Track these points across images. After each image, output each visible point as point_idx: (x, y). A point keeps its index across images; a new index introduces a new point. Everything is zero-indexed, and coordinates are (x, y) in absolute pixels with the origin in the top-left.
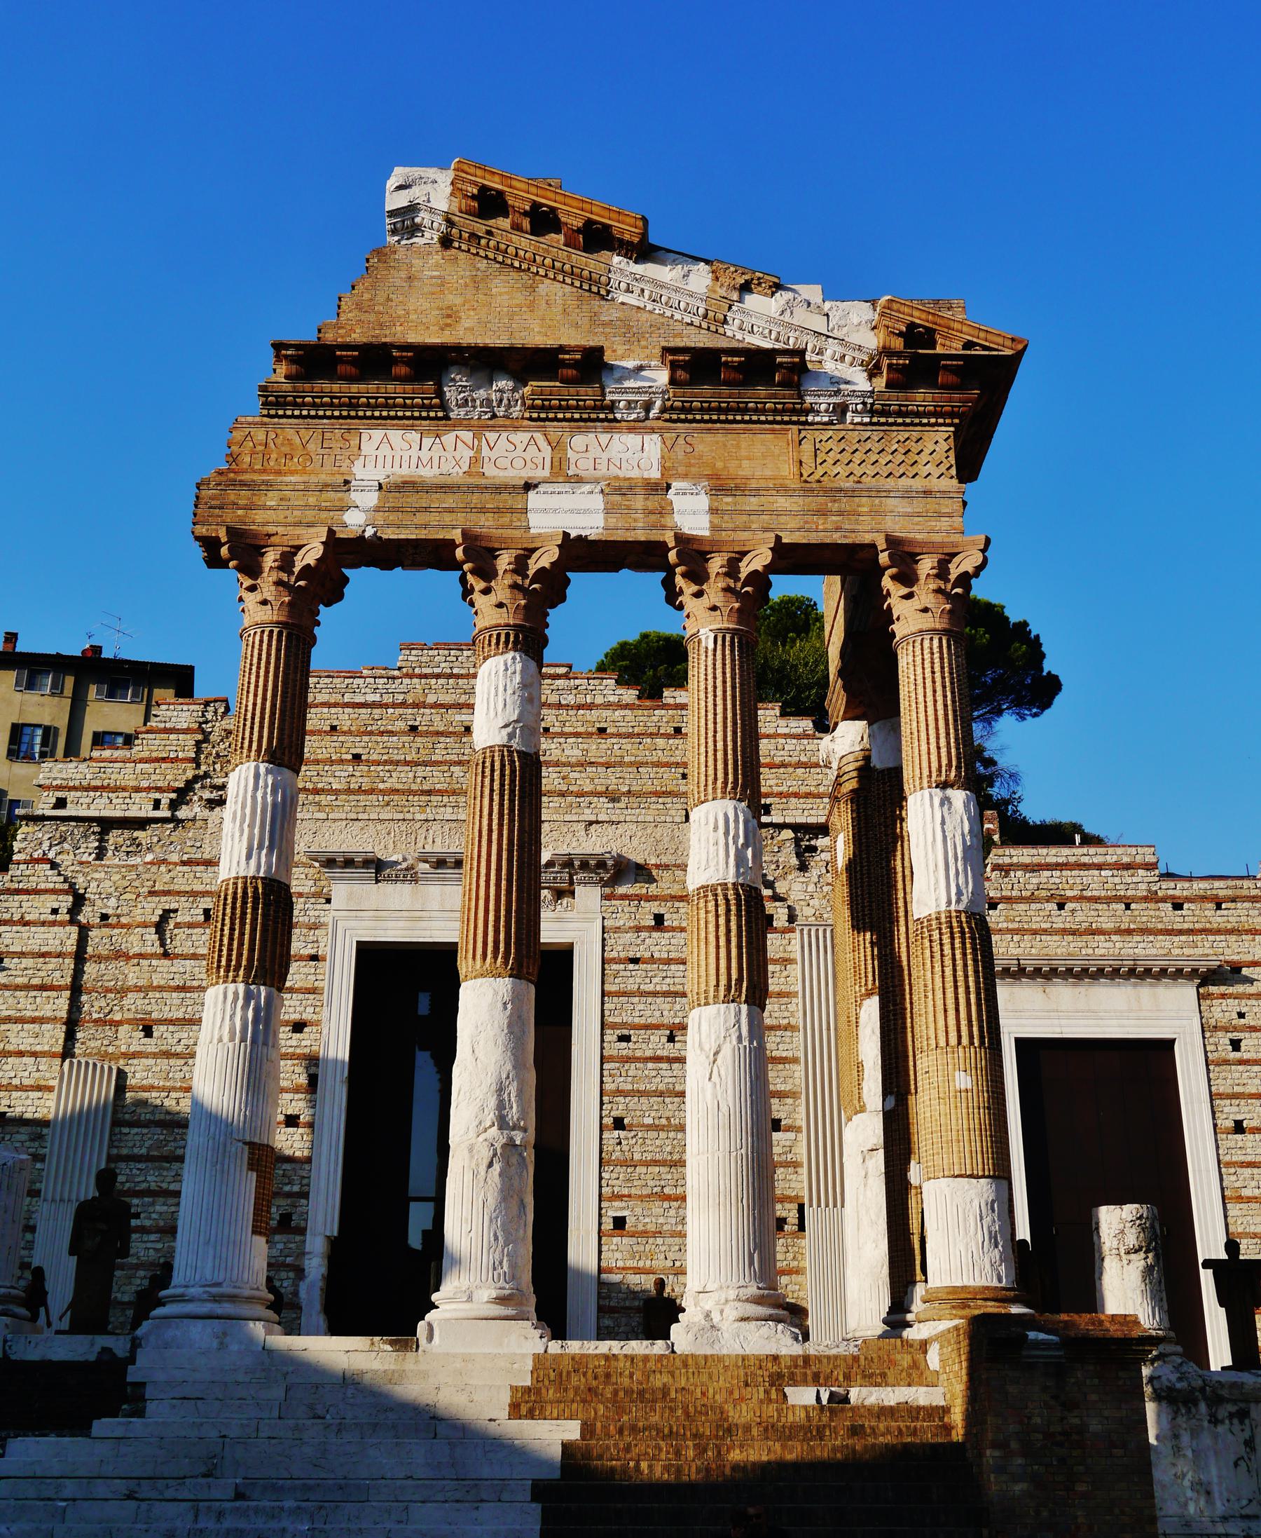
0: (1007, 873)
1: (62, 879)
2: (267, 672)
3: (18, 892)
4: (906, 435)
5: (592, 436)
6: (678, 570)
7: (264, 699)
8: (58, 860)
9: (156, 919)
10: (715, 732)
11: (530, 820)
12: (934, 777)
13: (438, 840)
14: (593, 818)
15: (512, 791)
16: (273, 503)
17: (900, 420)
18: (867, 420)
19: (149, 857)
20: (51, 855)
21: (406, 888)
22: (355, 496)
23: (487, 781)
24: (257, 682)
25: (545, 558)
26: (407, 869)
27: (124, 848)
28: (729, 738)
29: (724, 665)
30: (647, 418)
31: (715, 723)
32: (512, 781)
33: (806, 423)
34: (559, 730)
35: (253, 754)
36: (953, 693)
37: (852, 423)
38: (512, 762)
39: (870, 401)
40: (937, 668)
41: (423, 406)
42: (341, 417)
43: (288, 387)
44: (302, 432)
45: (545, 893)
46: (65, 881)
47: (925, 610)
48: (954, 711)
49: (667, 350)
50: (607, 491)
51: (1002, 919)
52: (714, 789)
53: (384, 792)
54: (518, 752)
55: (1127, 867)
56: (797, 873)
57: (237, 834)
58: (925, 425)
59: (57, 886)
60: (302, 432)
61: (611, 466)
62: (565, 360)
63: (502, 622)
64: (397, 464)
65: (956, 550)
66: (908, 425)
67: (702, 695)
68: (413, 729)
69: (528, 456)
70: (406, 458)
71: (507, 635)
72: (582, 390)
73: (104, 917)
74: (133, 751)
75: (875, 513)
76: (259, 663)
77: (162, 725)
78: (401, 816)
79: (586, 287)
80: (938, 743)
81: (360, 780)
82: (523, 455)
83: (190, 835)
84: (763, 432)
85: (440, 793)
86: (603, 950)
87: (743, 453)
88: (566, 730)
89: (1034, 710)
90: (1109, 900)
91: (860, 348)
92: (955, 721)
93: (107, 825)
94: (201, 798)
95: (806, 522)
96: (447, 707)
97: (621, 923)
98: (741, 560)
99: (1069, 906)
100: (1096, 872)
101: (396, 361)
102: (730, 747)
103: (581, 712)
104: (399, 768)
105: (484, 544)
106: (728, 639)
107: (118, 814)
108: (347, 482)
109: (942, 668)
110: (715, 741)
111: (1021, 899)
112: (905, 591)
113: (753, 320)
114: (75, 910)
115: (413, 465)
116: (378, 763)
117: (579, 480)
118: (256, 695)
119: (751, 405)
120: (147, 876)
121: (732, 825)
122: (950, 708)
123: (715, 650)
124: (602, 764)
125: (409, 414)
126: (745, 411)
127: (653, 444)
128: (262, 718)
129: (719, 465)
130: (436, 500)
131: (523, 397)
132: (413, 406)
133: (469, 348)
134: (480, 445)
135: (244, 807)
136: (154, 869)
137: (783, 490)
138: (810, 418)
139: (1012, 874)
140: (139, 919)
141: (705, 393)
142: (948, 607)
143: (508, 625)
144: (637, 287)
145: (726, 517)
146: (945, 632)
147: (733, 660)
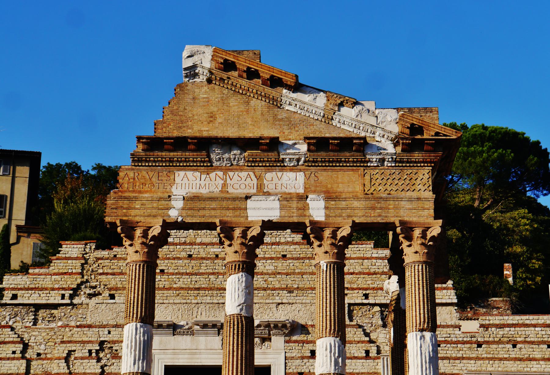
0: (487, 328)
1: (17, 336)
2: (139, 283)
4: (411, 171)
5: (274, 173)
6: (311, 236)
7: (138, 295)
8: (14, 326)
9: (65, 355)
10: (326, 307)
11: (250, 346)
12: (418, 327)
13: (204, 313)
14: (280, 301)
15: (242, 334)
16: (138, 206)
17: (408, 165)
18: (393, 165)
19: (60, 324)
20: (10, 323)
21: (188, 338)
22: (173, 203)
23: (232, 329)
24: (135, 287)
25: (255, 231)
26: (189, 329)
27: (47, 319)
28: (332, 310)
29: (330, 277)
30: (298, 165)
31: (326, 303)
32: (242, 330)
33: (367, 166)
34: (263, 256)
35: (134, 319)
36: (427, 289)
37: (387, 166)
38: (242, 321)
39: (395, 157)
40: (421, 279)
41: (201, 161)
42: (166, 166)
43: (143, 154)
44: (149, 173)
45: (257, 340)
46: (19, 337)
47: (416, 252)
48: (427, 297)
49: (306, 138)
50: (281, 199)
51: (484, 352)
52: (326, 332)
53: (176, 289)
54: (244, 317)
56: (382, 329)
57: (129, 354)
58: (419, 167)
59: (15, 340)
60: (149, 173)
61: (283, 187)
62: (262, 143)
63: (237, 260)
64: (191, 187)
65: (430, 226)
66: (411, 167)
67: (321, 291)
68: (190, 256)
69: (247, 183)
70: (194, 185)
71: (239, 265)
72: (270, 154)
73: (39, 355)
74: (51, 268)
75: (396, 208)
76: (135, 279)
77: (64, 256)
78: (185, 301)
79: (271, 102)
80: (420, 312)
81: (164, 283)
82: (245, 182)
83: (80, 312)
84: (348, 170)
85: (205, 289)
86: (286, 369)
87: (340, 180)
88: (267, 256)
89: (545, 192)
90: (539, 343)
91: (391, 132)
92: (427, 302)
93: (38, 307)
94: (85, 293)
95: (366, 213)
96: (207, 244)
97: (294, 355)
98: (338, 231)
99: (519, 346)
100: (533, 329)
101: (190, 143)
102: (332, 314)
103: (274, 246)
104: (184, 277)
105: (229, 225)
106: (332, 266)
107: (44, 302)
108: (170, 196)
109: (423, 278)
110: (326, 312)
111: (494, 342)
112: (408, 243)
113: (345, 119)
114: (24, 351)
115: (198, 188)
116: (173, 274)
117: (268, 194)
118: (134, 293)
119: (343, 159)
120: (60, 333)
121: (333, 348)
122: (425, 296)
123: (326, 271)
124: (284, 274)
125: (195, 164)
126: (340, 162)
127: (301, 176)
128: (138, 303)
129: (329, 186)
130: (208, 204)
131: (244, 157)
132: (197, 161)
133: (221, 138)
134: (226, 178)
135: (131, 342)
136: (63, 329)
137: (356, 198)
138: (369, 164)
139: (490, 329)
140: (57, 355)
141: (322, 155)
142: (426, 251)
143: (239, 261)
144: (294, 103)
145: (332, 211)
146: (424, 262)
147: (334, 275)
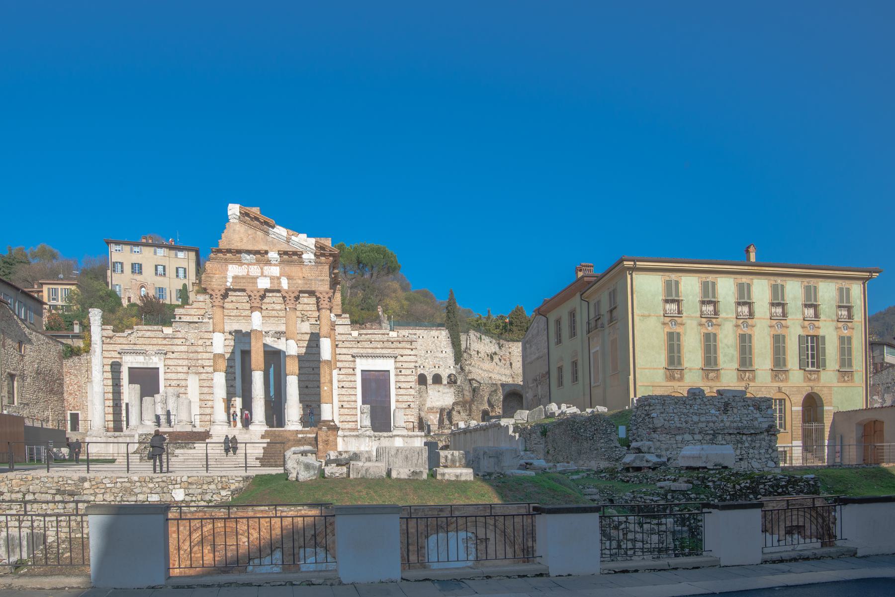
3: (175, 338)
22: (228, 279)
55: (384, 334)
111: (364, 341)
117: (266, 276)
137: (299, 279)
